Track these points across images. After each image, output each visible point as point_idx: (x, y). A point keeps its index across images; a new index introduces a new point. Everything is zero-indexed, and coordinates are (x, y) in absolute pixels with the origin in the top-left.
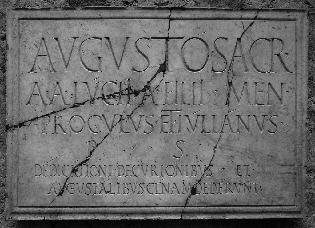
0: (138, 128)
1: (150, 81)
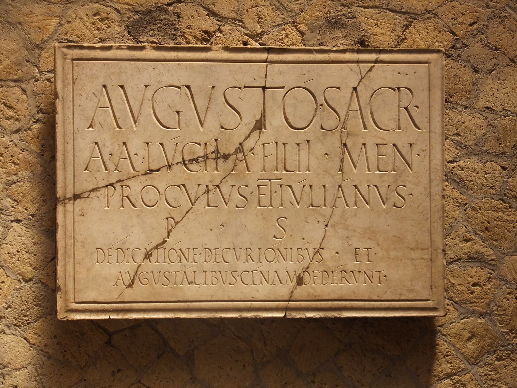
0: (228, 201)
1: (244, 141)
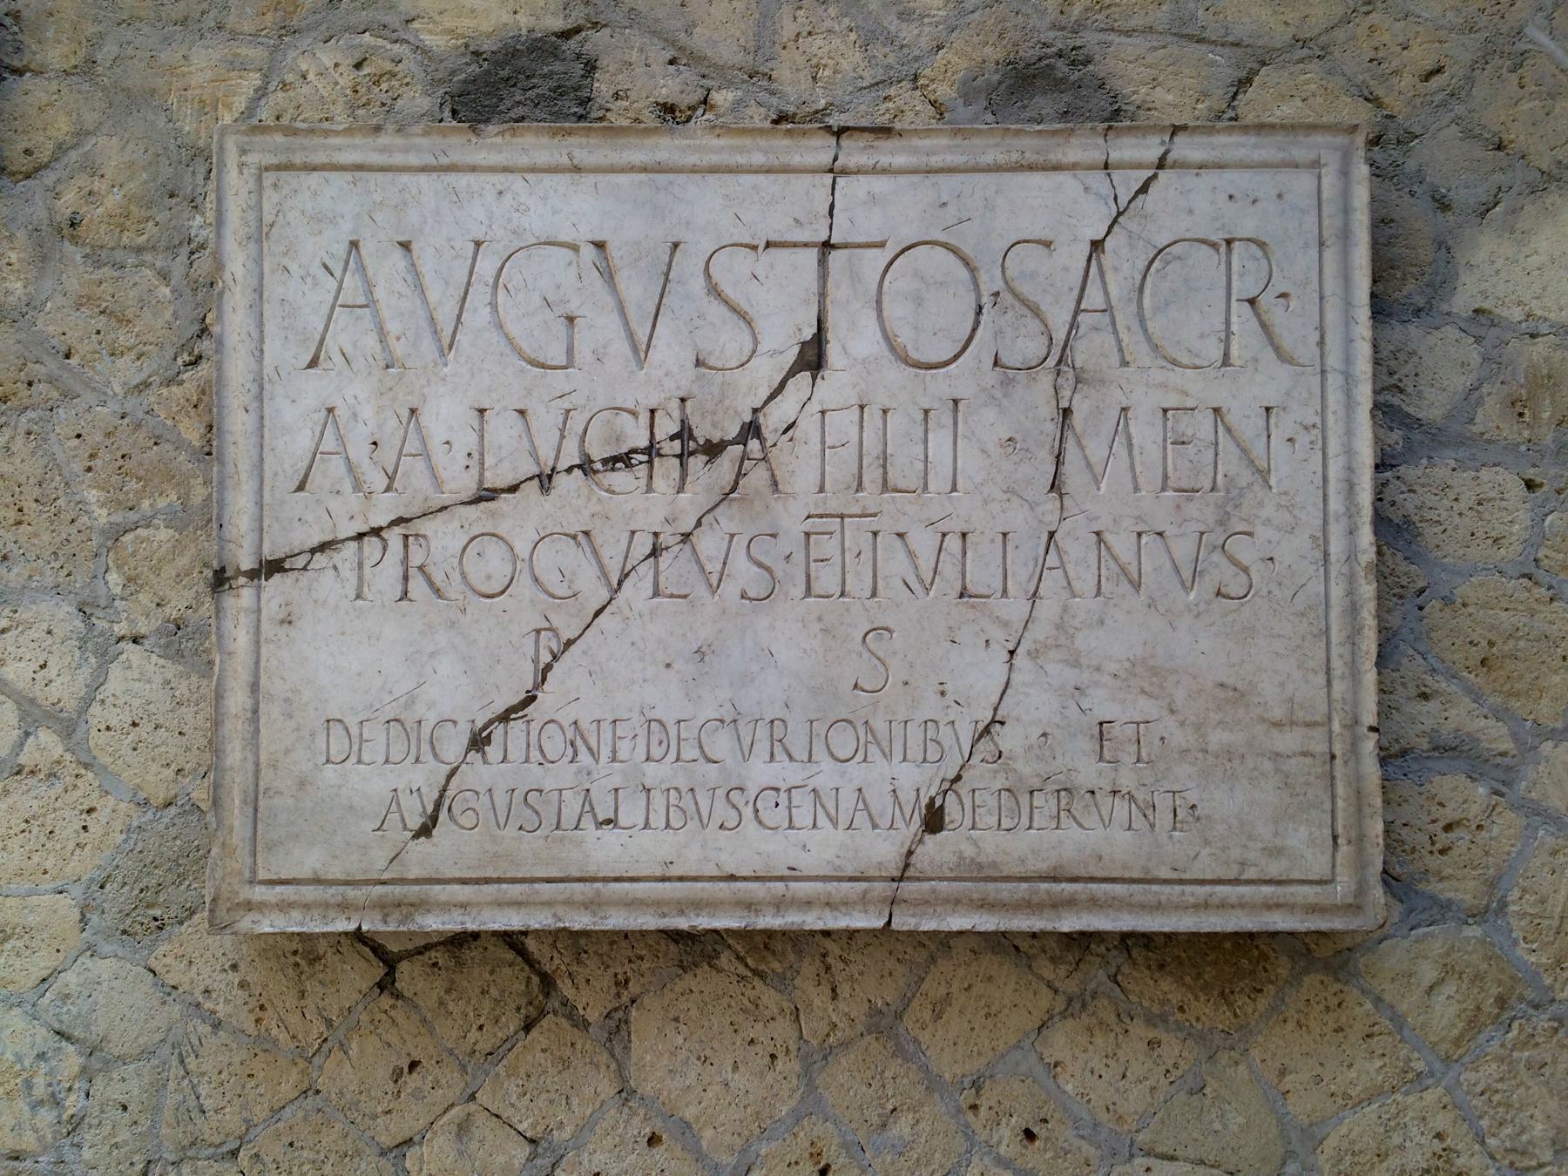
0: (720, 580)
1: (766, 403)
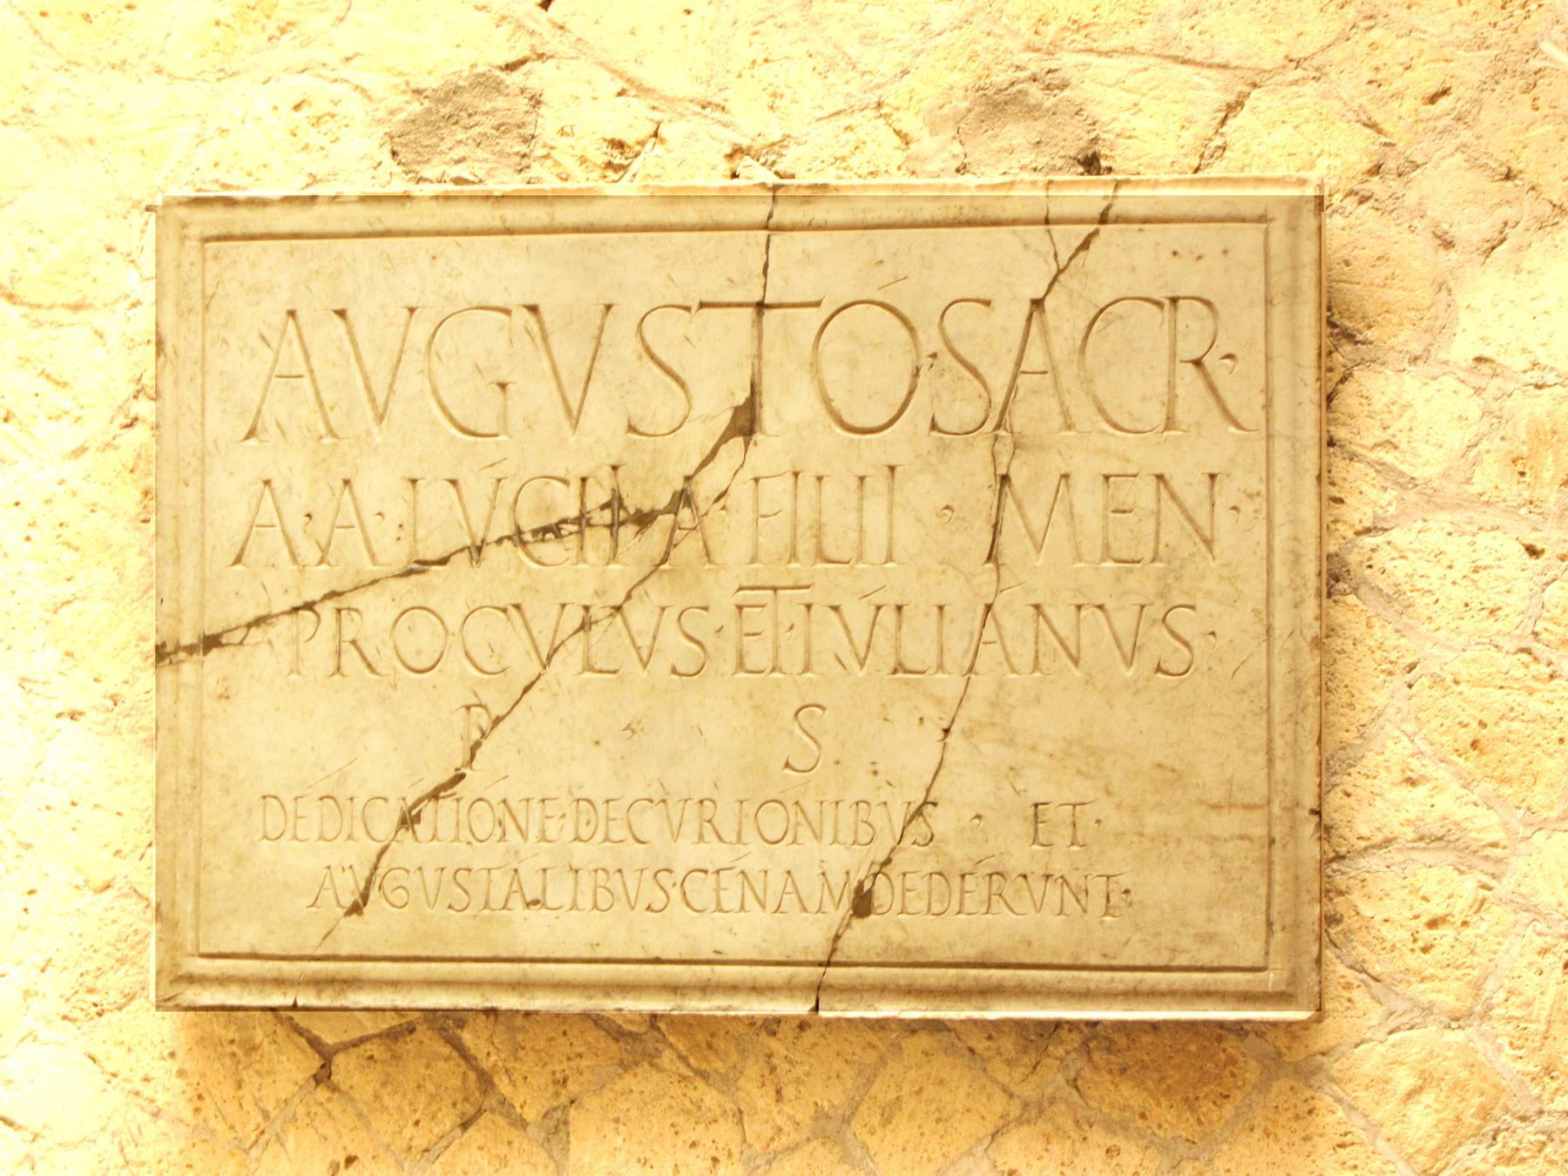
0: (650, 655)
